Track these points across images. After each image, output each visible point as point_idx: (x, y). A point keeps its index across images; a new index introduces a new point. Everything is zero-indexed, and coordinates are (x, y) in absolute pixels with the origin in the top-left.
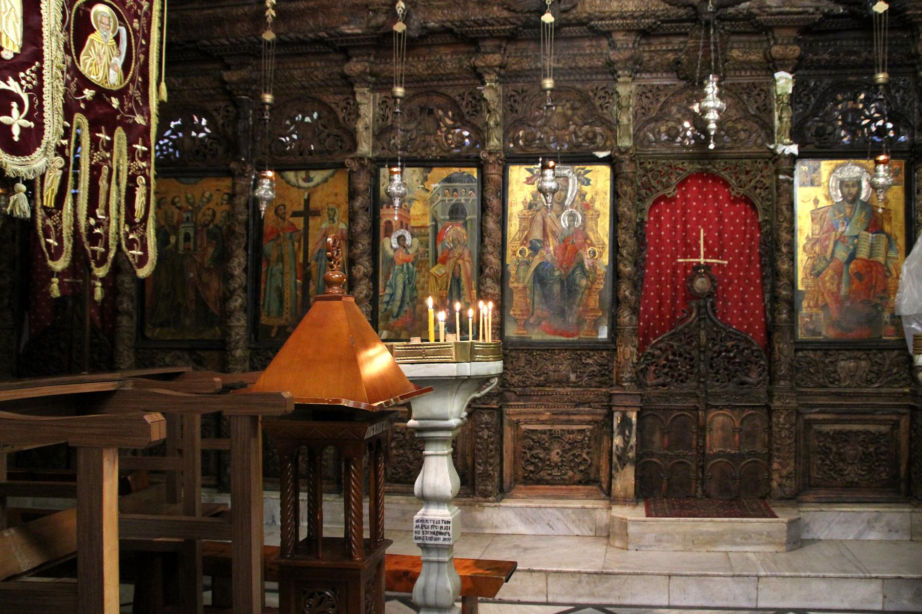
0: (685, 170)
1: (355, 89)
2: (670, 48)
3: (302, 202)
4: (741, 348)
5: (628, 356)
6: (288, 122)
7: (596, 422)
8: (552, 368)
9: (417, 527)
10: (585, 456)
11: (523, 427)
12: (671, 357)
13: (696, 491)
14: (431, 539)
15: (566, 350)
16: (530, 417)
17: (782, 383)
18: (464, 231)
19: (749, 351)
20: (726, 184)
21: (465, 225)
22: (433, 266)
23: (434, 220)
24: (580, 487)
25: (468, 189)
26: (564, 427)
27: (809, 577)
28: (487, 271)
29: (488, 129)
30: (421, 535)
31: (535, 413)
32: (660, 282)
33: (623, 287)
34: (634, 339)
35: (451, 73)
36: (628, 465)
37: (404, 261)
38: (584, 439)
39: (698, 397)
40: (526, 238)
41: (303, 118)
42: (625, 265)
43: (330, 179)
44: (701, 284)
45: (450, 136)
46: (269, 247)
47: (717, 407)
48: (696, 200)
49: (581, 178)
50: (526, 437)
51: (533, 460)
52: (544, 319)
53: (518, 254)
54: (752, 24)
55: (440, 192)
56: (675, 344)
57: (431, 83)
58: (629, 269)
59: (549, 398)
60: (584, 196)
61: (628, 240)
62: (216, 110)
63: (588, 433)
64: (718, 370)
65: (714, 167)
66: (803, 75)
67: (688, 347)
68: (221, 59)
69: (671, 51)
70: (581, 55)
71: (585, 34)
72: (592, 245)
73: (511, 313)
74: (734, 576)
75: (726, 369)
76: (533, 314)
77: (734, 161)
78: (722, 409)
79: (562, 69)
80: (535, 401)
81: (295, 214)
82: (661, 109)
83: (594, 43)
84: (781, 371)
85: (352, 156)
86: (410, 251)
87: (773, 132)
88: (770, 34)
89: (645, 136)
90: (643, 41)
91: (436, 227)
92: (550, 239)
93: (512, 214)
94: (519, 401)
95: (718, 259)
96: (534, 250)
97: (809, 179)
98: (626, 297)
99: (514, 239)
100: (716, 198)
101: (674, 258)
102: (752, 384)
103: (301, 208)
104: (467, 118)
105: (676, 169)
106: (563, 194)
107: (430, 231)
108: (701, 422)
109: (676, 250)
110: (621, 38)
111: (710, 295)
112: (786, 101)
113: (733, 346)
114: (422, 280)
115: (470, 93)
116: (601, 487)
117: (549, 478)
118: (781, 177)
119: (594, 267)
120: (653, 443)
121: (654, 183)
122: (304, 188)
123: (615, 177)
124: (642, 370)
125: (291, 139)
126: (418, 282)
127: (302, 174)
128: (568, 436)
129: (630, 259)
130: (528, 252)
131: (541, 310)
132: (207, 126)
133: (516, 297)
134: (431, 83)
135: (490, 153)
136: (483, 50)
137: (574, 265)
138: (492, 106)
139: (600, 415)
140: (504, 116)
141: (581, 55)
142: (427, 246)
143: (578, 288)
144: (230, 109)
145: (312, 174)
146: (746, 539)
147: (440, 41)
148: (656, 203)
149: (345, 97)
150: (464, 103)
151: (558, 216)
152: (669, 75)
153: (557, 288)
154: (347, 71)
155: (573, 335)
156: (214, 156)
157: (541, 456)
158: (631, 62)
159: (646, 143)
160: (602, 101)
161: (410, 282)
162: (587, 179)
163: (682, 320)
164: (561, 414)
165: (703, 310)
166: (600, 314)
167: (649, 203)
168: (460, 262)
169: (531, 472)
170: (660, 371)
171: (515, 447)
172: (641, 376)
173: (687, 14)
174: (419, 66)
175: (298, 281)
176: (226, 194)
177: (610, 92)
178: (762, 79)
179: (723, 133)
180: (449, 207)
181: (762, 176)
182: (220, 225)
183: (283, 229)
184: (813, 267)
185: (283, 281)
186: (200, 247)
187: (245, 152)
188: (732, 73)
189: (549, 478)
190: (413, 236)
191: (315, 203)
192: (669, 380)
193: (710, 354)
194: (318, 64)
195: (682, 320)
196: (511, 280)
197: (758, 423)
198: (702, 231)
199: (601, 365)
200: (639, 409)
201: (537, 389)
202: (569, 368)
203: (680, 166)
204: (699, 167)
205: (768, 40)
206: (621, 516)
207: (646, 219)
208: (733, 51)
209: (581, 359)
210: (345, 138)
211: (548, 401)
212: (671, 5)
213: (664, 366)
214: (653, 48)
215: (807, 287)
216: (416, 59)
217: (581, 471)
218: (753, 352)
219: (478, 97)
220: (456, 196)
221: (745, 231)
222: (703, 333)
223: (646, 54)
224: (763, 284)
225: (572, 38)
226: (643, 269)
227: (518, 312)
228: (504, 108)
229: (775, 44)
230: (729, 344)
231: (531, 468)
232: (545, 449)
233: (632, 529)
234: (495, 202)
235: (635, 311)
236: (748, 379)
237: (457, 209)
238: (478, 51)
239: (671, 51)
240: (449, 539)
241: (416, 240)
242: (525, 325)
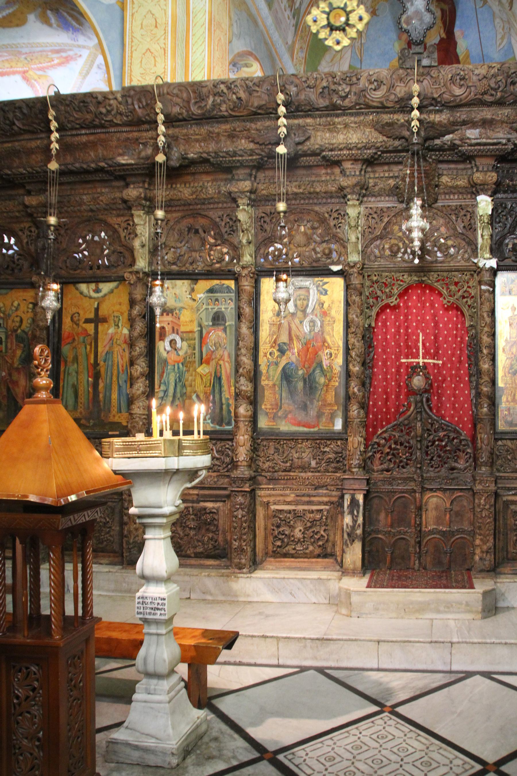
0: (405, 282)
1: (133, 212)
2: (391, 175)
3: (93, 310)
4: (451, 437)
5: (356, 445)
6: (81, 241)
7: (332, 503)
8: (296, 455)
9: (139, 603)
10: (322, 532)
11: (273, 507)
12: (393, 446)
13: (414, 564)
14: (150, 614)
15: (307, 440)
16: (278, 498)
17: (483, 469)
18: (224, 335)
19: (458, 441)
20: (440, 294)
21: (225, 330)
22: (199, 366)
23: (200, 325)
24: (319, 560)
25: (227, 299)
26: (306, 507)
27: (493, 643)
28: (241, 370)
29: (242, 246)
30: (142, 610)
31: (282, 495)
32: (386, 379)
33: (353, 384)
34: (361, 430)
35: (212, 198)
36: (356, 541)
37: (175, 362)
38: (322, 518)
39: (415, 481)
40: (275, 342)
41: (93, 237)
42: (354, 365)
43: (115, 291)
44: (418, 381)
45: (212, 253)
46: (66, 349)
47: (431, 490)
48: (416, 307)
49: (320, 288)
50: (275, 516)
51: (281, 537)
52: (290, 412)
53: (268, 355)
54: (456, 153)
55: (204, 302)
56: (397, 435)
57: (195, 207)
58: (357, 368)
59: (294, 482)
60: (323, 305)
61: (357, 344)
62: (21, 230)
63: (325, 513)
64: (433, 457)
65: (429, 279)
66: (502, 198)
67: (407, 437)
68: (22, 186)
69: (392, 177)
70: (318, 181)
71: (320, 163)
72: (329, 347)
73: (263, 407)
74: (431, 642)
75: (439, 456)
76: (281, 408)
77: (445, 274)
78: (435, 491)
79: (302, 193)
80: (282, 484)
81: (87, 321)
82: (385, 228)
83: (329, 171)
84: (482, 458)
85: (130, 270)
86: (181, 353)
87: (477, 248)
88: (473, 162)
89: (372, 252)
90: (369, 169)
91: (201, 332)
92: (295, 342)
93: (263, 320)
94: (269, 484)
95: (434, 359)
96: (282, 352)
97: (507, 289)
98: (354, 393)
99: (265, 343)
100: (432, 306)
101: (398, 359)
102: (460, 469)
103: (92, 316)
104: (226, 237)
105: (397, 280)
106: (305, 303)
107: (196, 335)
108: (418, 504)
109: (400, 351)
110: (350, 166)
111: (426, 391)
112: (486, 221)
113: (444, 436)
114: (190, 378)
115: (228, 215)
116: (336, 560)
117: (294, 552)
118: (483, 287)
119: (331, 367)
120: (379, 521)
121: (379, 293)
122: (94, 298)
123: (347, 287)
124: (369, 458)
125: (84, 255)
126: (187, 380)
127: (93, 286)
128: (309, 515)
129: (358, 360)
130: (277, 354)
131: (287, 405)
132: (16, 244)
133: (267, 393)
134: (195, 207)
135: (243, 268)
136: (236, 177)
137: (314, 365)
138: (245, 226)
139: (335, 496)
140: (256, 235)
141: (318, 181)
142: (194, 349)
143: (317, 385)
144: (33, 229)
145: (101, 285)
146: (448, 608)
147: (201, 170)
148: (383, 309)
149: (126, 218)
150: (223, 224)
151: (301, 322)
152: (391, 198)
153: (300, 385)
154: (125, 197)
155: (314, 427)
156: (20, 270)
157: (287, 533)
158: (358, 188)
159: (373, 258)
160: (335, 222)
161: (180, 381)
162: (324, 290)
163: (404, 413)
164: (303, 496)
165: (419, 405)
166: (336, 408)
167: (375, 310)
168: (221, 362)
169: (279, 547)
170: (385, 458)
171: (265, 525)
172: (369, 463)
173: (401, 145)
174: (185, 192)
175: (90, 379)
176: (31, 303)
177: (342, 213)
178: (468, 202)
179: (436, 249)
180: (212, 315)
181: (469, 287)
182: (27, 330)
183: (78, 334)
184: (511, 366)
185: (77, 379)
186: (11, 349)
187: (44, 267)
188: (443, 197)
189: (294, 552)
190: (182, 340)
192: (392, 466)
193: (425, 443)
194: (103, 190)
195: (404, 413)
196: (263, 378)
197: (465, 504)
198: (421, 335)
199: (336, 453)
200: (365, 492)
201: (283, 474)
202: (310, 455)
203: (401, 278)
204: (416, 279)
205: (472, 167)
206: (346, 587)
207: (373, 325)
208: (444, 177)
209: (320, 448)
210: (127, 254)
211: (293, 484)
212: (388, 137)
213: (388, 454)
214: (377, 175)
215: (506, 384)
216: (183, 186)
217: (320, 546)
218: (461, 441)
219: (234, 219)
220: (218, 305)
221: (456, 334)
222: (419, 424)
224: (470, 382)
225: (310, 167)
226: (372, 368)
227: (269, 406)
228: (255, 228)
229: (477, 171)
230: (441, 434)
231: (279, 543)
232: (290, 527)
233: (354, 599)
234: (247, 310)
235: (363, 406)
236: (456, 465)
237: (218, 317)
238: (233, 179)
239: (392, 177)
240: (165, 615)
241: (185, 344)
242: (275, 417)
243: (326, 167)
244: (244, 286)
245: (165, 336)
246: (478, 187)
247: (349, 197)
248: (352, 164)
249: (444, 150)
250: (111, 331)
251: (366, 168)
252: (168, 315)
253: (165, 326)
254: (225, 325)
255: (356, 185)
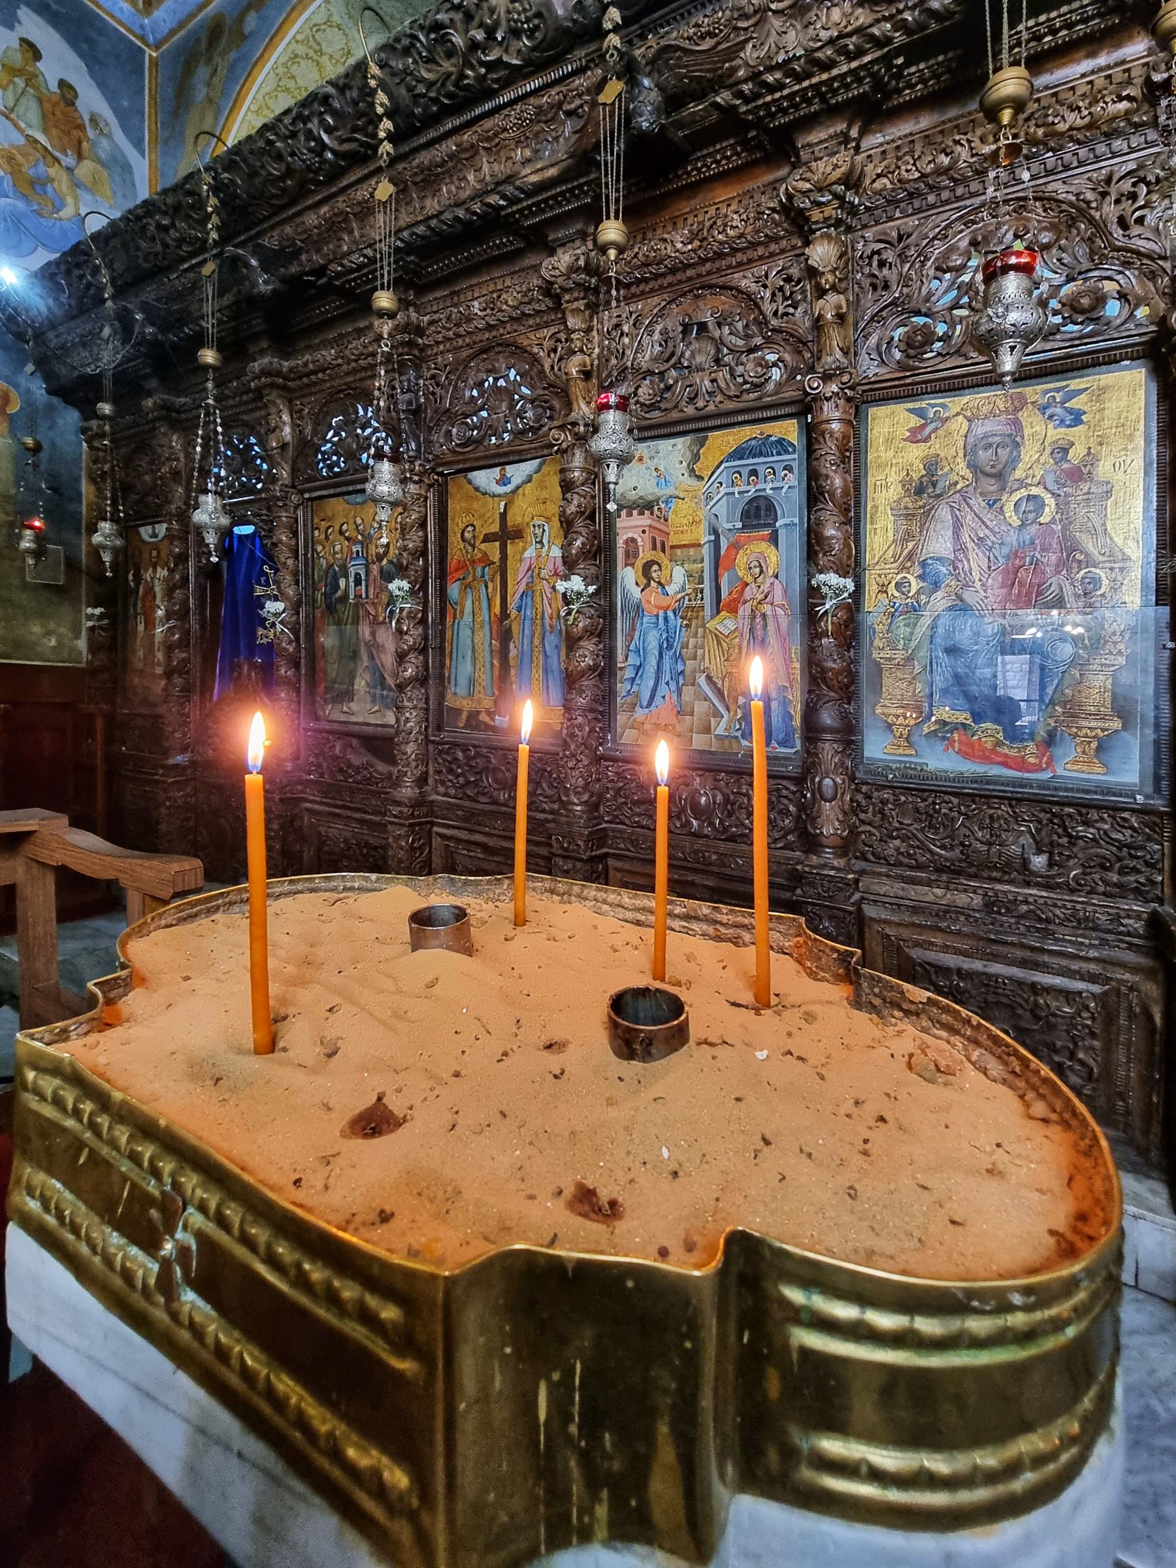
37: (659, 608)
81: (488, 538)
86: (671, 589)
91: (716, 544)
93: (875, 507)
103: (495, 528)
107: (706, 552)
145: (510, 470)
168: (767, 609)
191: (514, 519)
244: (828, 421)
245: (636, 556)
250: (530, 553)
252: (641, 513)
253: (636, 536)
254: (773, 525)
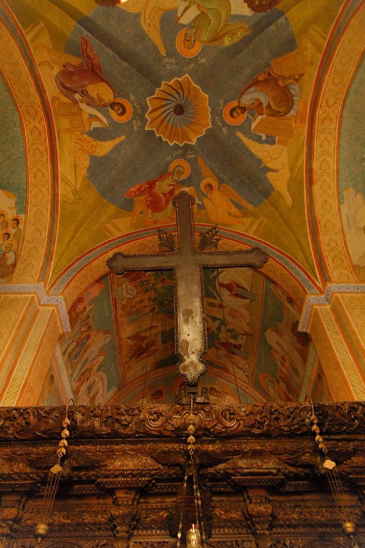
70: (88, 512)
71: (93, 492)
79: (69, 525)
83: (101, 501)
88: (245, 494)
90: (142, 500)
110: (123, 495)
152: (163, 532)
205: (245, 499)
223: (143, 512)
225: (81, 497)
229: (251, 502)
243: (99, 497)
246: (254, 519)
247: (118, 528)
248: (126, 493)
249: (217, 480)
251: (139, 499)
255: (127, 515)
